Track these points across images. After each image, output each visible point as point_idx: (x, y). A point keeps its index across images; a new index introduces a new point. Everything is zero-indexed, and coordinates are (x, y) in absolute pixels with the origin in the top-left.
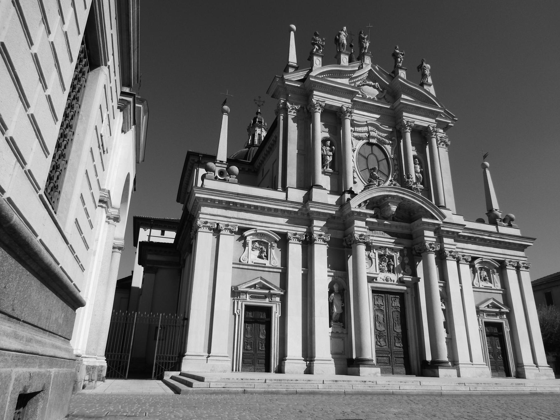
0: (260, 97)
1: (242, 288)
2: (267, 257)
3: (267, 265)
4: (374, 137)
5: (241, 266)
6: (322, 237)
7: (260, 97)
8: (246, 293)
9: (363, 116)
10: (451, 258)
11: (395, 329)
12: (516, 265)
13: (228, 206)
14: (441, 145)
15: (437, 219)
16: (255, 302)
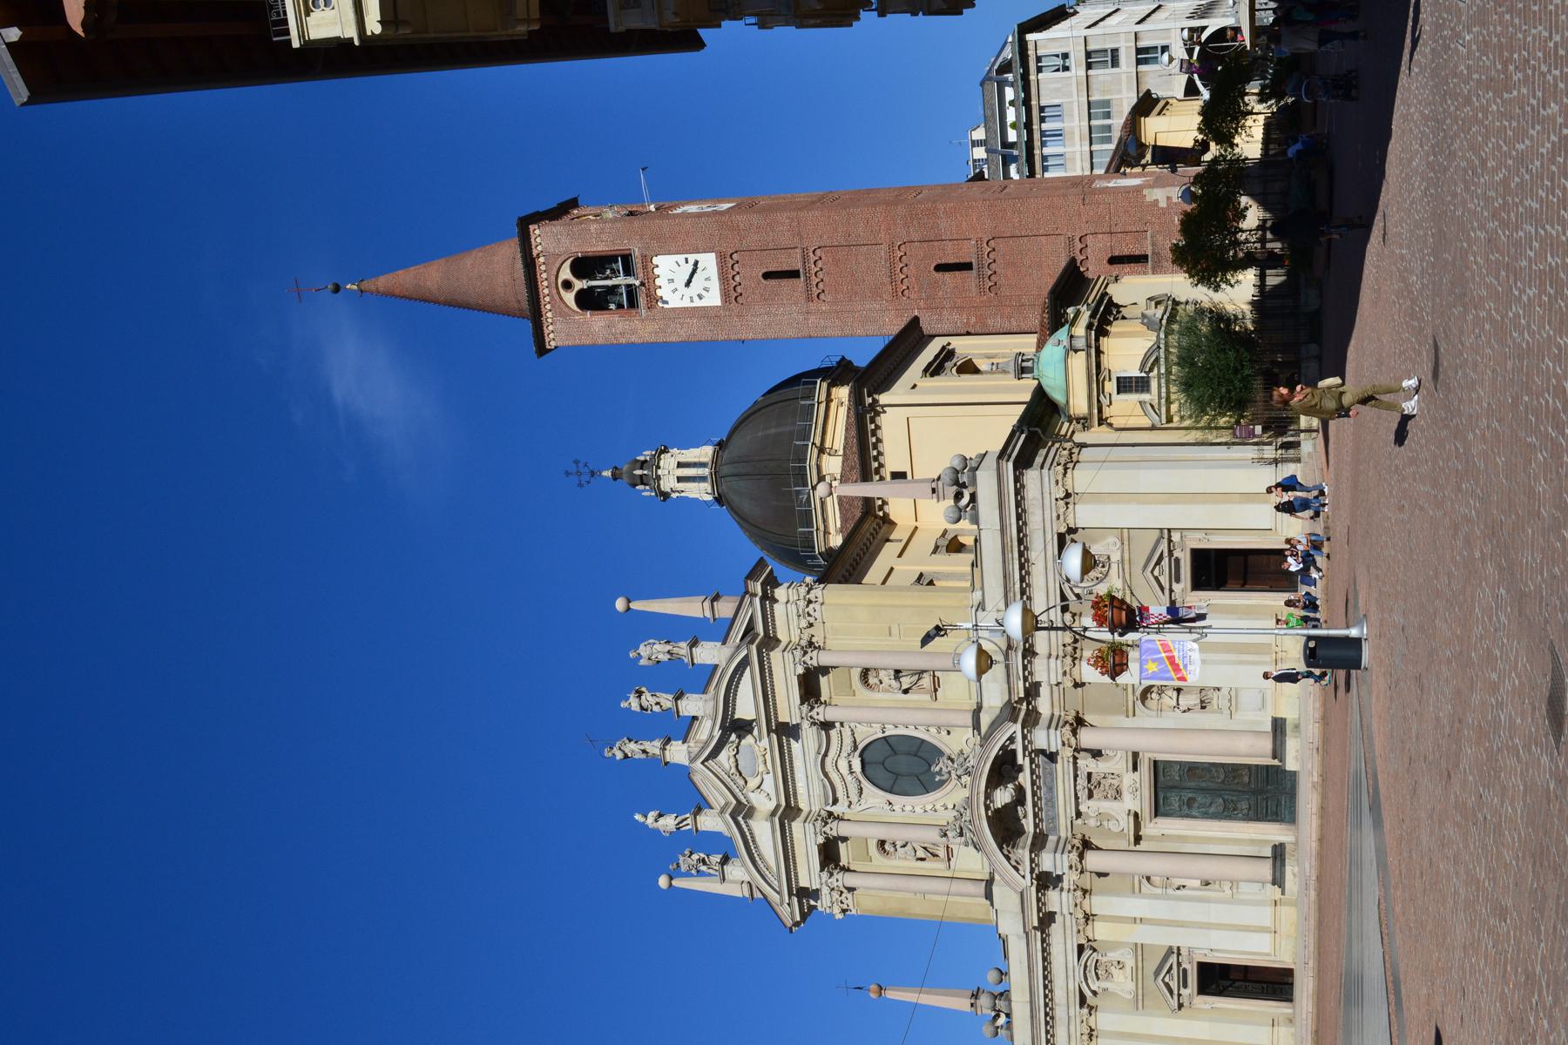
0: (567, 474)
1: (1176, 1005)
2: (1119, 962)
3: (1134, 966)
4: (850, 766)
5: (1140, 997)
6: (1078, 902)
7: (567, 474)
8: (1179, 995)
9: (810, 777)
10: (1076, 671)
11: (1220, 780)
12: (1061, 503)
13: (1050, 1017)
14: (817, 614)
15: (1015, 732)
16: (1192, 981)
